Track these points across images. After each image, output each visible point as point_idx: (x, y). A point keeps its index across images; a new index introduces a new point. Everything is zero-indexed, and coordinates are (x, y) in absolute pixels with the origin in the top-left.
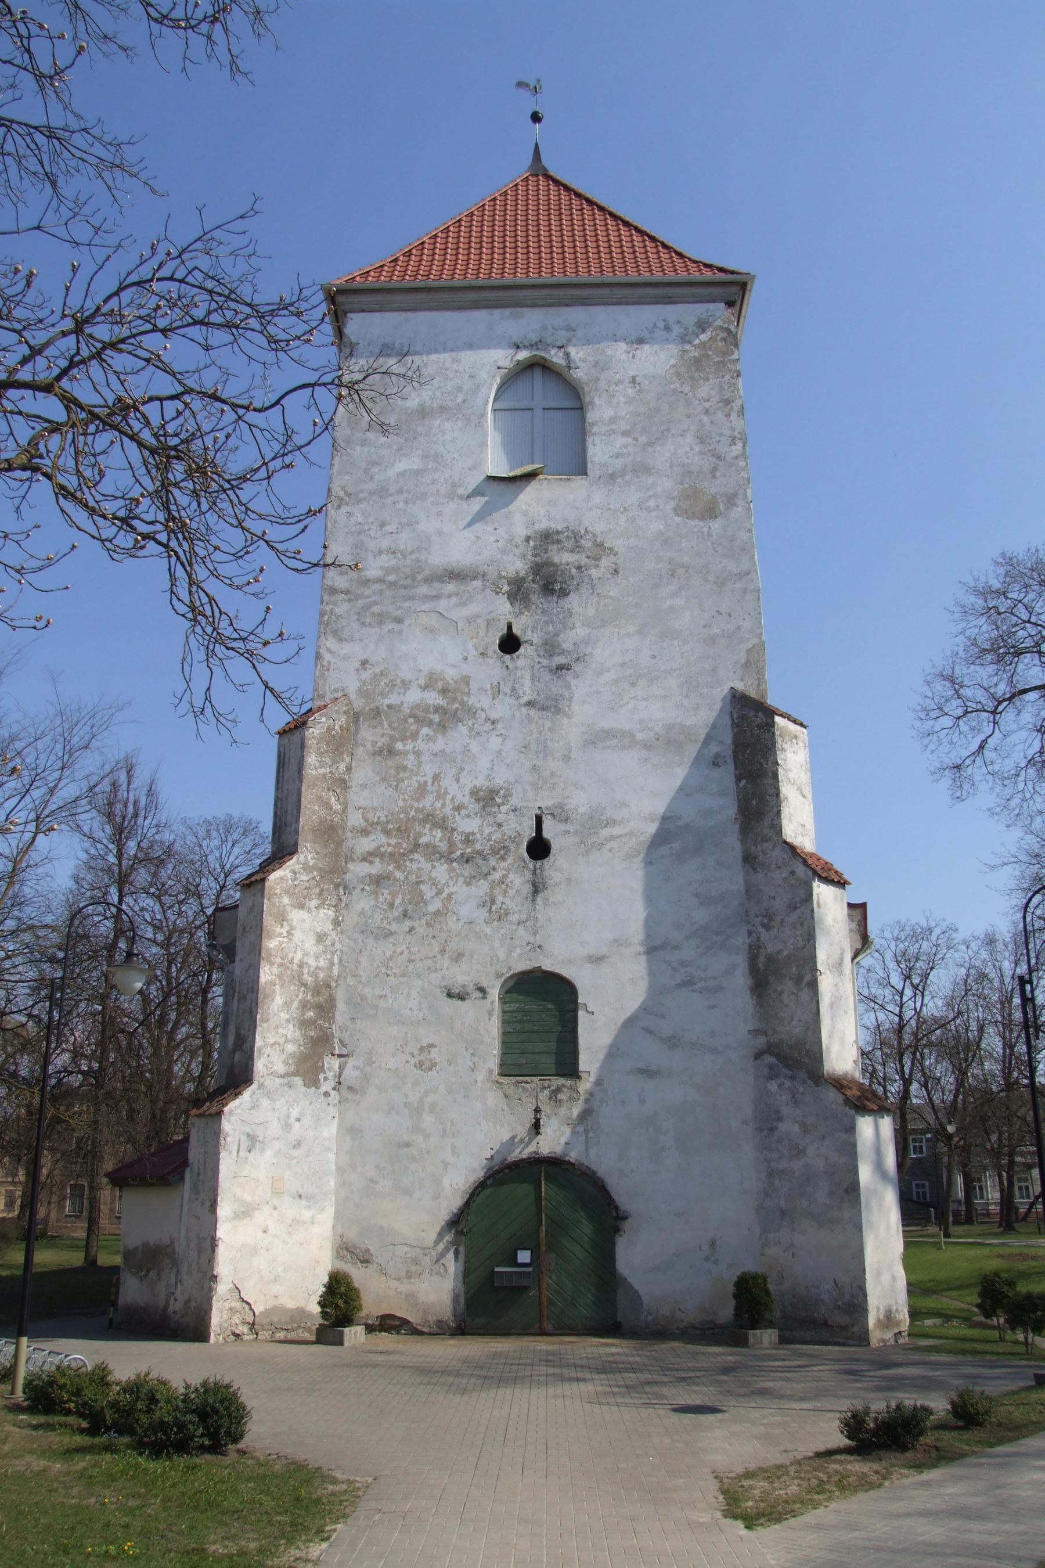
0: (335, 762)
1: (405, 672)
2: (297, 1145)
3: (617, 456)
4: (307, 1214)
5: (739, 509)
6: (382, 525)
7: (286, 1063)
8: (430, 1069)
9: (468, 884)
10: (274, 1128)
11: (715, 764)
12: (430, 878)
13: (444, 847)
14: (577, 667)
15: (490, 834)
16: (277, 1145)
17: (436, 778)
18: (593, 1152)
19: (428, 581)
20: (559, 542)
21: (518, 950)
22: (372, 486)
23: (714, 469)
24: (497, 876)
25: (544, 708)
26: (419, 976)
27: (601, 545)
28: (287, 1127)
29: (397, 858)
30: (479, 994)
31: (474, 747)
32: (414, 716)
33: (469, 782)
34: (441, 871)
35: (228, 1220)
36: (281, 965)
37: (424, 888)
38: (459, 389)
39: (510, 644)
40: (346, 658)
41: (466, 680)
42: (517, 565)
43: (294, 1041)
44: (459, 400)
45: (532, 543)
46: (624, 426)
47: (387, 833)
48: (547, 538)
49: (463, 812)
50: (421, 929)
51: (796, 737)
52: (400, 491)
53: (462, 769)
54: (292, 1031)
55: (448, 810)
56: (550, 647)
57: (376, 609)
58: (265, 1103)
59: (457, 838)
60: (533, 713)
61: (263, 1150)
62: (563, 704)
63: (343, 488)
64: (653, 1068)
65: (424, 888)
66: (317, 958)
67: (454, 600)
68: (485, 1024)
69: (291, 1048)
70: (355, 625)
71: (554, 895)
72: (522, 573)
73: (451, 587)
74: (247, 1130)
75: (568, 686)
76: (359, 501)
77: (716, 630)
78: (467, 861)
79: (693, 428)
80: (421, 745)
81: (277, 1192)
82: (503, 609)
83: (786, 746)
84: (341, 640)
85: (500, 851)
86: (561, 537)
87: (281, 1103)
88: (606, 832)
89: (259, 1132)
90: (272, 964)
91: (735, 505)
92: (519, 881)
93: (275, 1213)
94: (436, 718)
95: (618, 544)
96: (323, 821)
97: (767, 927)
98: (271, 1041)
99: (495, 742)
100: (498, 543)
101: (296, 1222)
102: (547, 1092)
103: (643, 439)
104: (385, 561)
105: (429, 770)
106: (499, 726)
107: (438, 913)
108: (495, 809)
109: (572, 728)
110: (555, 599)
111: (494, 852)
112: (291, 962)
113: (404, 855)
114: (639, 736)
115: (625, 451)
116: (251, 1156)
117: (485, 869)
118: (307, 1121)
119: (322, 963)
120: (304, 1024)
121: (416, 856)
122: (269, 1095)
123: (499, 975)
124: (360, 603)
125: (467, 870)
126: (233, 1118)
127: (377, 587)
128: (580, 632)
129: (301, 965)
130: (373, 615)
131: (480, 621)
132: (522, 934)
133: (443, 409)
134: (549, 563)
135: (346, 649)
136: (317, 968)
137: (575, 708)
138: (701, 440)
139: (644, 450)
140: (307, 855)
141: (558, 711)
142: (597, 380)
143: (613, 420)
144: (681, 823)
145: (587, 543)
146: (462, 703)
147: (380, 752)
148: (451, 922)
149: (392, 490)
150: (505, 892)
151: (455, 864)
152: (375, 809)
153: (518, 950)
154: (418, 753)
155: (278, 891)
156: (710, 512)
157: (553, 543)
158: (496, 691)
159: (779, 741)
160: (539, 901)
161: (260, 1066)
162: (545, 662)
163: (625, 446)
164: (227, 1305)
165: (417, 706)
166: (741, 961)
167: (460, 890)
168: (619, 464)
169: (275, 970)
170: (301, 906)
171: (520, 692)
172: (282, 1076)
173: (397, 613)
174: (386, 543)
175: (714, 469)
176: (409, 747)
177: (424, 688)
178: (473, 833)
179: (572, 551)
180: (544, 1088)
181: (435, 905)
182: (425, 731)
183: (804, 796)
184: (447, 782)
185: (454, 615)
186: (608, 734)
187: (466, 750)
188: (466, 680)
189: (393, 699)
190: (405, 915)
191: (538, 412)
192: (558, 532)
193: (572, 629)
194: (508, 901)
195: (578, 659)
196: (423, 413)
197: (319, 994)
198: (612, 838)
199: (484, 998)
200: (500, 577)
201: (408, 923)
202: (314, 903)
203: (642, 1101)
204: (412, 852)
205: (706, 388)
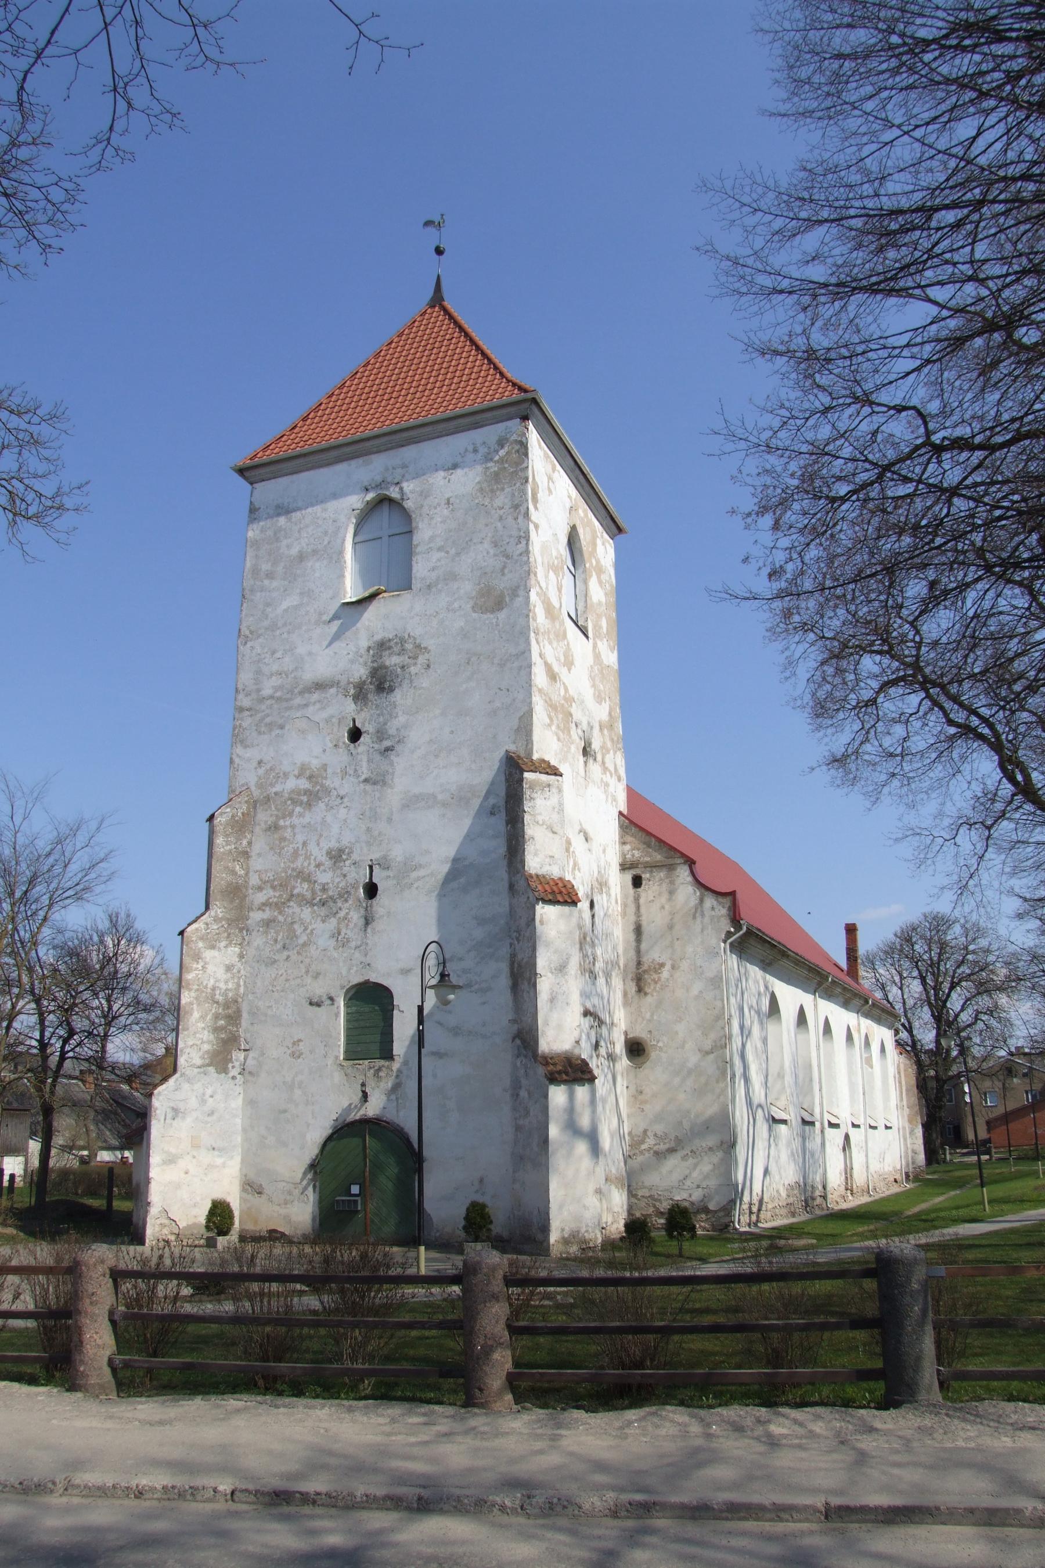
0: (238, 839)
1: (286, 766)
2: (211, 1113)
4: (219, 1161)
6: (273, 653)
7: (202, 1057)
9: (323, 921)
10: (193, 1102)
11: (492, 814)
13: (308, 895)
14: (398, 748)
17: (304, 844)
18: (401, 1114)
19: (301, 693)
20: (390, 648)
22: (266, 623)
23: (504, 567)
24: (342, 914)
25: (375, 783)
26: (293, 991)
27: (418, 647)
28: (203, 1102)
29: (279, 906)
31: (329, 819)
32: (291, 799)
33: (326, 845)
34: (306, 913)
35: (158, 1165)
37: (296, 926)
38: (326, 533)
39: (355, 735)
40: (249, 760)
41: (324, 767)
42: (360, 672)
43: (209, 1042)
46: (439, 542)
47: (273, 888)
48: (383, 646)
50: (294, 957)
52: (285, 625)
53: (321, 836)
54: (207, 1036)
55: (312, 868)
56: (381, 734)
57: (268, 720)
58: (186, 1086)
59: (317, 887)
60: (368, 787)
61: (184, 1118)
62: (388, 778)
63: (248, 627)
65: (296, 926)
66: (226, 982)
67: (318, 706)
69: (206, 1047)
70: (254, 734)
71: (378, 925)
73: (316, 696)
75: (392, 764)
76: (259, 637)
77: (498, 704)
80: (295, 820)
81: (196, 1146)
83: (534, 795)
84: (246, 747)
85: (345, 895)
86: (392, 644)
87: (198, 1086)
88: (414, 875)
89: (181, 1106)
90: (190, 990)
92: (356, 917)
95: (430, 643)
96: (229, 884)
99: (342, 812)
100: (344, 659)
101: (211, 1167)
103: (453, 551)
104: (275, 681)
105: (300, 838)
106: (346, 800)
107: (304, 945)
109: (394, 796)
111: (341, 896)
112: (206, 987)
118: (218, 1097)
119: (230, 986)
120: (216, 1030)
122: (189, 1081)
123: (342, 987)
124: (259, 716)
125: (323, 911)
127: (269, 702)
128: (402, 719)
129: (214, 989)
133: (315, 552)
135: (248, 753)
137: (396, 780)
139: (453, 560)
140: (218, 910)
142: (422, 506)
143: (432, 539)
144: (466, 863)
145: (409, 646)
146: (322, 786)
148: (312, 948)
149: (280, 624)
152: (266, 871)
154: (293, 827)
156: (499, 604)
158: (344, 773)
159: (527, 793)
160: (369, 930)
162: (376, 746)
163: (439, 560)
164: (158, 1222)
165: (293, 791)
166: (504, 967)
167: (318, 926)
168: (434, 575)
169: (193, 994)
170: (213, 947)
173: (281, 721)
174: (275, 667)
175: (504, 567)
176: (288, 823)
177: (297, 777)
181: (303, 939)
182: (298, 809)
184: (312, 847)
185: (316, 718)
186: (418, 798)
187: (324, 821)
188: (324, 767)
189: (278, 788)
191: (385, 539)
196: (301, 557)
198: (418, 879)
200: (349, 683)
201: (286, 953)
202: (223, 944)
205: (502, 497)
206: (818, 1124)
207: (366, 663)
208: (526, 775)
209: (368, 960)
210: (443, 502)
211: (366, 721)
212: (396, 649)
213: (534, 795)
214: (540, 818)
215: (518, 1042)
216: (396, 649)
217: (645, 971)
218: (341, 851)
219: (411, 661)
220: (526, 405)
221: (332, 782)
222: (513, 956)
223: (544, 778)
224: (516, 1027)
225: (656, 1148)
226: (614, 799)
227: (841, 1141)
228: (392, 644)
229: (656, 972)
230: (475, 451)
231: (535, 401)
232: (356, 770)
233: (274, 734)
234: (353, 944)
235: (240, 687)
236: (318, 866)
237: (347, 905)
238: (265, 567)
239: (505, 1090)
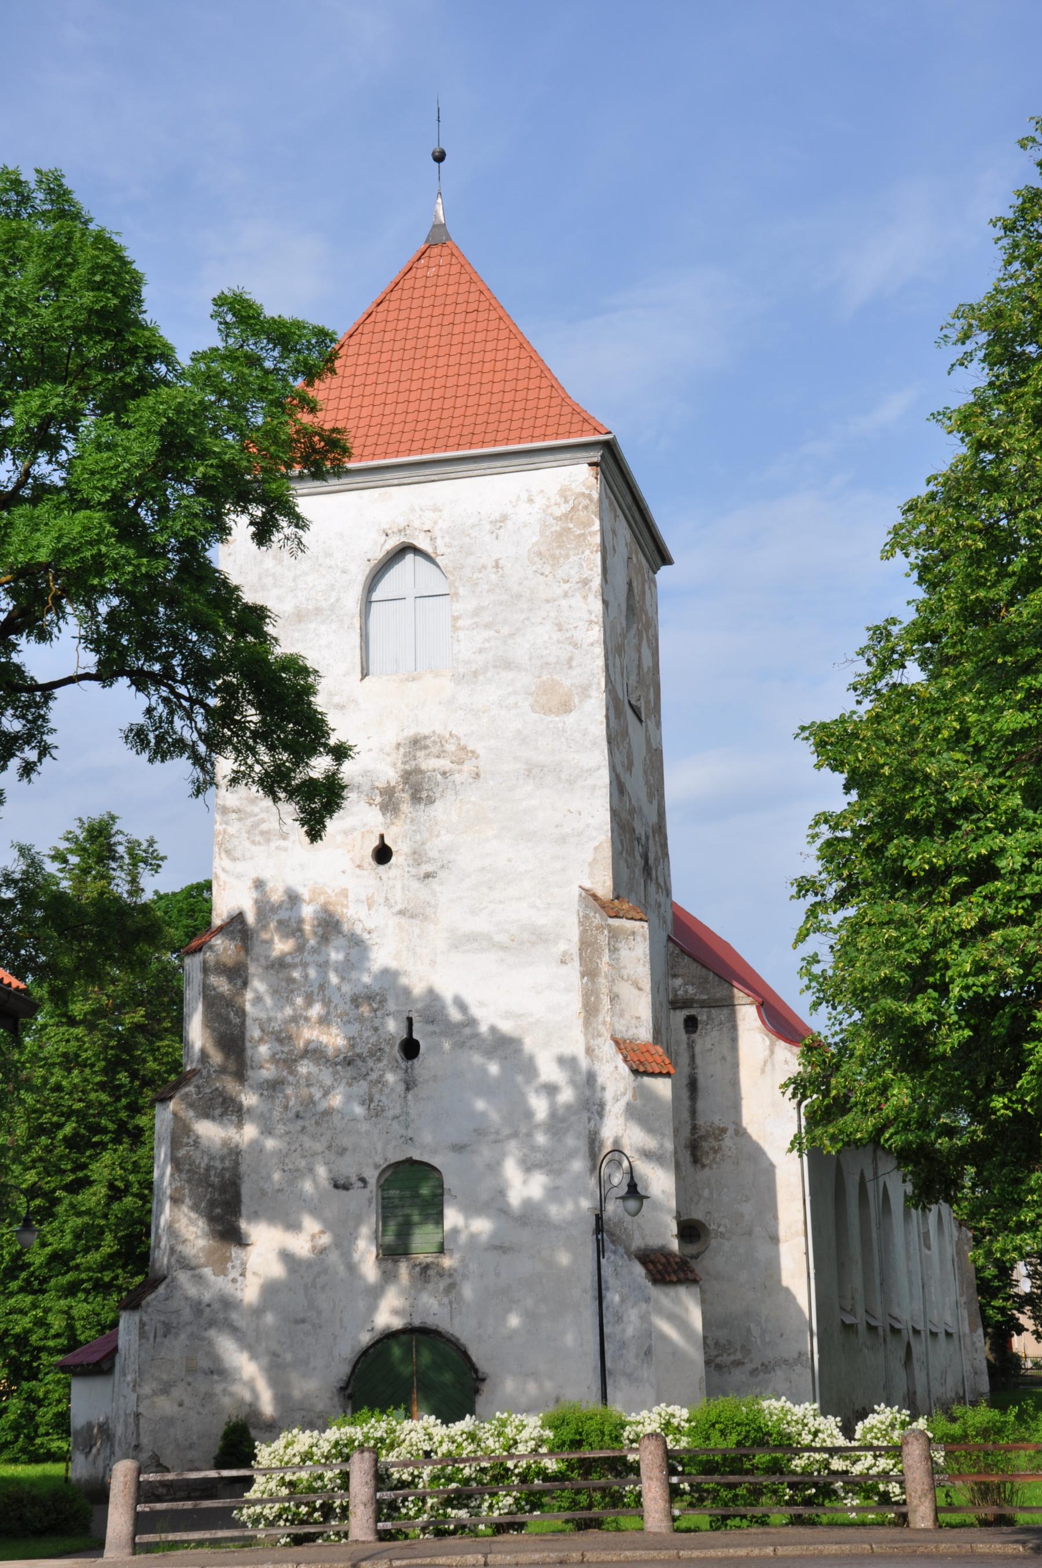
3: (480, 651)
5: (593, 701)
11: (563, 962)
12: (318, 1081)
14: (442, 874)
15: (368, 1038)
16: (189, 1329)
18: (456, 1321)
20: (426, 747)
21: (393, 1143)
23: (570, 660)
24: (374, 1076)
25: (412, 917)
36: (189, 1171)
39: (383, 854)
40: (239, 877)
41: (344, 893)
44: (332, 600)
45: (402, 750)
48: (417, 743)
50: (311, 1128)
51: (633, 933)
56: (417, 856)
57: (264, 827)
60: (403, 920)
61: (177, 1335)
64: (507, 1244)
70: (247, 844)
72: (393, 784)
74: (162, 1318)
75: (434, 893)
79: (553, 614)
83: (620, 945)
84: (235, 859)
85: (377, 1052)
86: (428, 742)
91: (589, 697)
93: (189, 1389)
95: (479, 747)
103: (505, 630)
110: (422, 807)
111: (372, 1054)
112: (199, 1167)
114: (497, 938)
115: (487, 645)
116: (166, 1341)
117: (364, 1071)
119: (227, 1164)
124: (249, 822)
125: (350, 1071)
126: (150, 1310)
128: (446, 838)
129: (208, 1168)
130: (262, 833)
131: (355, 834)
132: (395, 1125)
134: (418, 771)
135: (239, 867)
136: (223, 1169)
141: (426, 918)
143: (477, 612)
145: (451, 747)
147: (272, 966)
150: (381, 1091)
151: (339, 1067)
153: (393, 1143)
156: (566, 708)
157: (421, 749)
162: (414, 871)
163: (488, 640)
171: (392, 901)
175: (570, 660)
179: (438, 757)
183: (640, 989)
186: (472, 938)
188: (344, 893)
190: (298, 1116)
191: (410, 600)
192: (425, 738)
193: (438, 836)
194: (384, 1099)
195: (442, 867)
197: (225, 1192)
199: (365, 1187)
201: (300, 1123)
202: (218, 1112)
203: (498, 1275)
206: (880, 1330)
209: (410, 1133)
210: (490, 564)
212: (435, 750)
213: (620, 945)
214: (625, 972)
216: (435, 750)
217: (701, 1137)
219: (455, 767)
225: (719, 1360)
226: (665, 922)
227: (902, 1354)
229: (717, 1139)
232: (387, 899)
233: (273, 845)
234: (390, 1113)
237: (381, 1065)
239: (584, 1291)
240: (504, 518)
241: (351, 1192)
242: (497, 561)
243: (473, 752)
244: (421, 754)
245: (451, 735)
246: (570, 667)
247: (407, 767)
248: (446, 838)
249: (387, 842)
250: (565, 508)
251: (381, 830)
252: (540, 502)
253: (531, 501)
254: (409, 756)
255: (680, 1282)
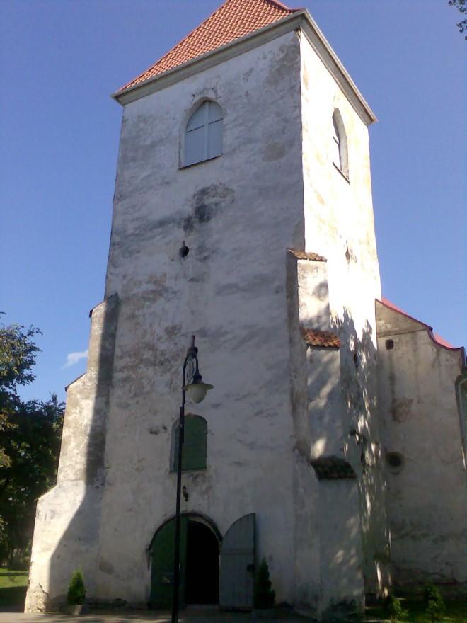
3: (237, 138)
6: (134, 207)
7: (75, 474)
8: (142, 470)
11: (277, 292)
13: (152, 359)
15: (172, 349)
19: (151, 229)
24: (174, 370)
27: (227, 189)
29: (133, 368)
30: (163, 430)
32: (144, 298)
34: (150, 371)
39: (185, 251)
41: (165, 275)
42: (189, 210)
45: (196, 197)
47: (130, 356)
48: (204, 192)
49: (161, 340)
52: (142, 188)
57: (130, 249)
58: (62, 494)
65: (144, 380)
68: (165, 444)
70: (122, 259)
72: (191, 215)
73: (159, 230)
74: (51, 508)
78: (162, 364)
82: (179, 234)
83: (305, 275)
86: (210, 190)
88: (222, 339)
94: (151, 296)
95: (235, 187)
97: (296, 377)
98: (68, 464)
102: (191, 478)
103: (250, 125)
104: (137, 224)
107: (149, 392)
108: (175, 336)
112: (81, 425)
113: (136, 366)
116: (52, 521)
121: (141, 365)
126: (43, 503)
128: (216, 237)
133: (161, 141)
134: (204, 206)
138: (278, 115)
151: (156, 367)
154: (144, 315)
155: (74, 392)
156: (281, 154)
158: (176, 278)
159: (300, 273)
161: (61, 476)
162: (198, 257)
163: (241, 132)
166: (286, 397)
172: (72, 481)
176: (141, 313)
177: (148, 283)
178: (164, 350)
180: (190, 476)
182: (147, 303)
188: (165, 275)
189: (136, 291)
192: (208, 188)
196: (153, 145)
198: (225, 342)
199: (166, 432)
201: (136, 399)
204: (139, 364)
207: (192, 206)
208: (299, 261)
211: (192, 242)
215: (297, 451)
216: (213, 193)
218: (174, 328)
219: (222, 199)
220: (299, 20)
221: (168, 283)
222: (293, 389)
223: (313, 263)
224: (295, 441)
228: (210, 190)
230: (265, 58)
231: (303, 17)
235: (114, 230)
236: (159, 339)
237: (177, 363)
238: (130, 154)
240: (251, 70)
241: (159, 435)
242: (247, 92)
243: (231, 190)
244: (205, 197)
245: (221, 184)
246: (284, 134)
247: (198, 205)
248: (216, 237)
249: (186, 245)
250: (282, 55)
251: (184, 239)
252: (269, 56)
253: (265, 58)
254: (200, 199)
255: (340, 477)
